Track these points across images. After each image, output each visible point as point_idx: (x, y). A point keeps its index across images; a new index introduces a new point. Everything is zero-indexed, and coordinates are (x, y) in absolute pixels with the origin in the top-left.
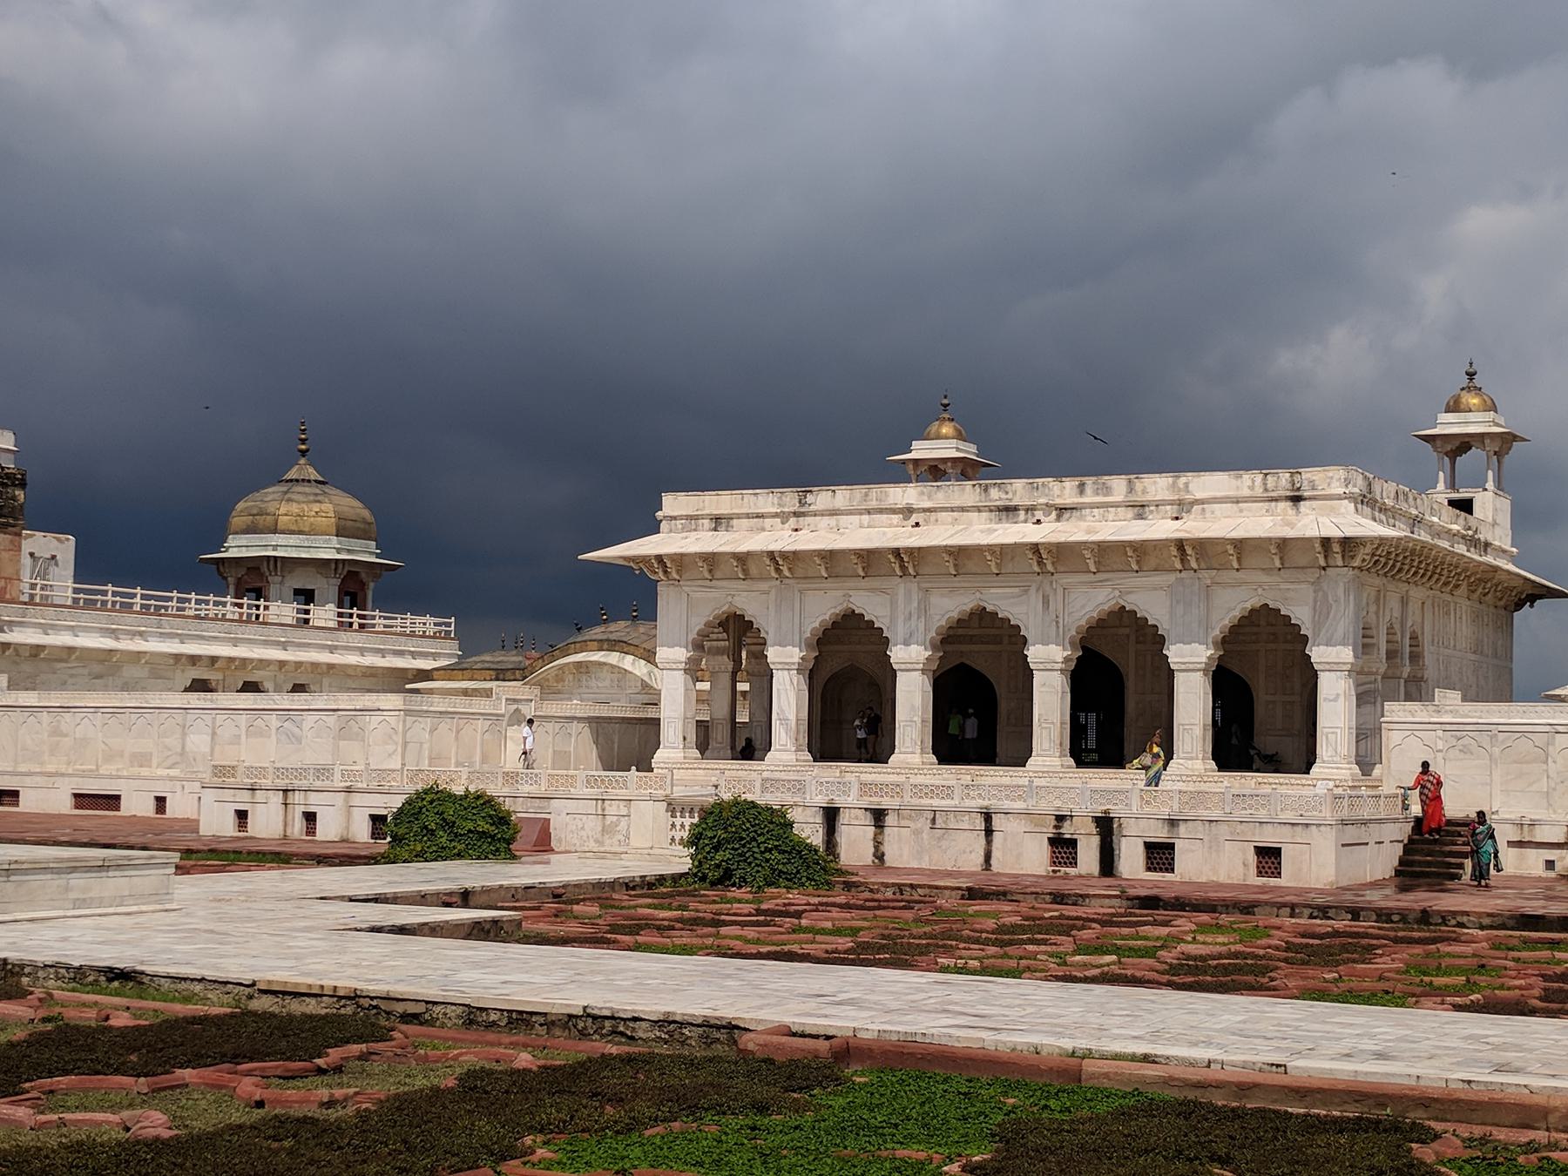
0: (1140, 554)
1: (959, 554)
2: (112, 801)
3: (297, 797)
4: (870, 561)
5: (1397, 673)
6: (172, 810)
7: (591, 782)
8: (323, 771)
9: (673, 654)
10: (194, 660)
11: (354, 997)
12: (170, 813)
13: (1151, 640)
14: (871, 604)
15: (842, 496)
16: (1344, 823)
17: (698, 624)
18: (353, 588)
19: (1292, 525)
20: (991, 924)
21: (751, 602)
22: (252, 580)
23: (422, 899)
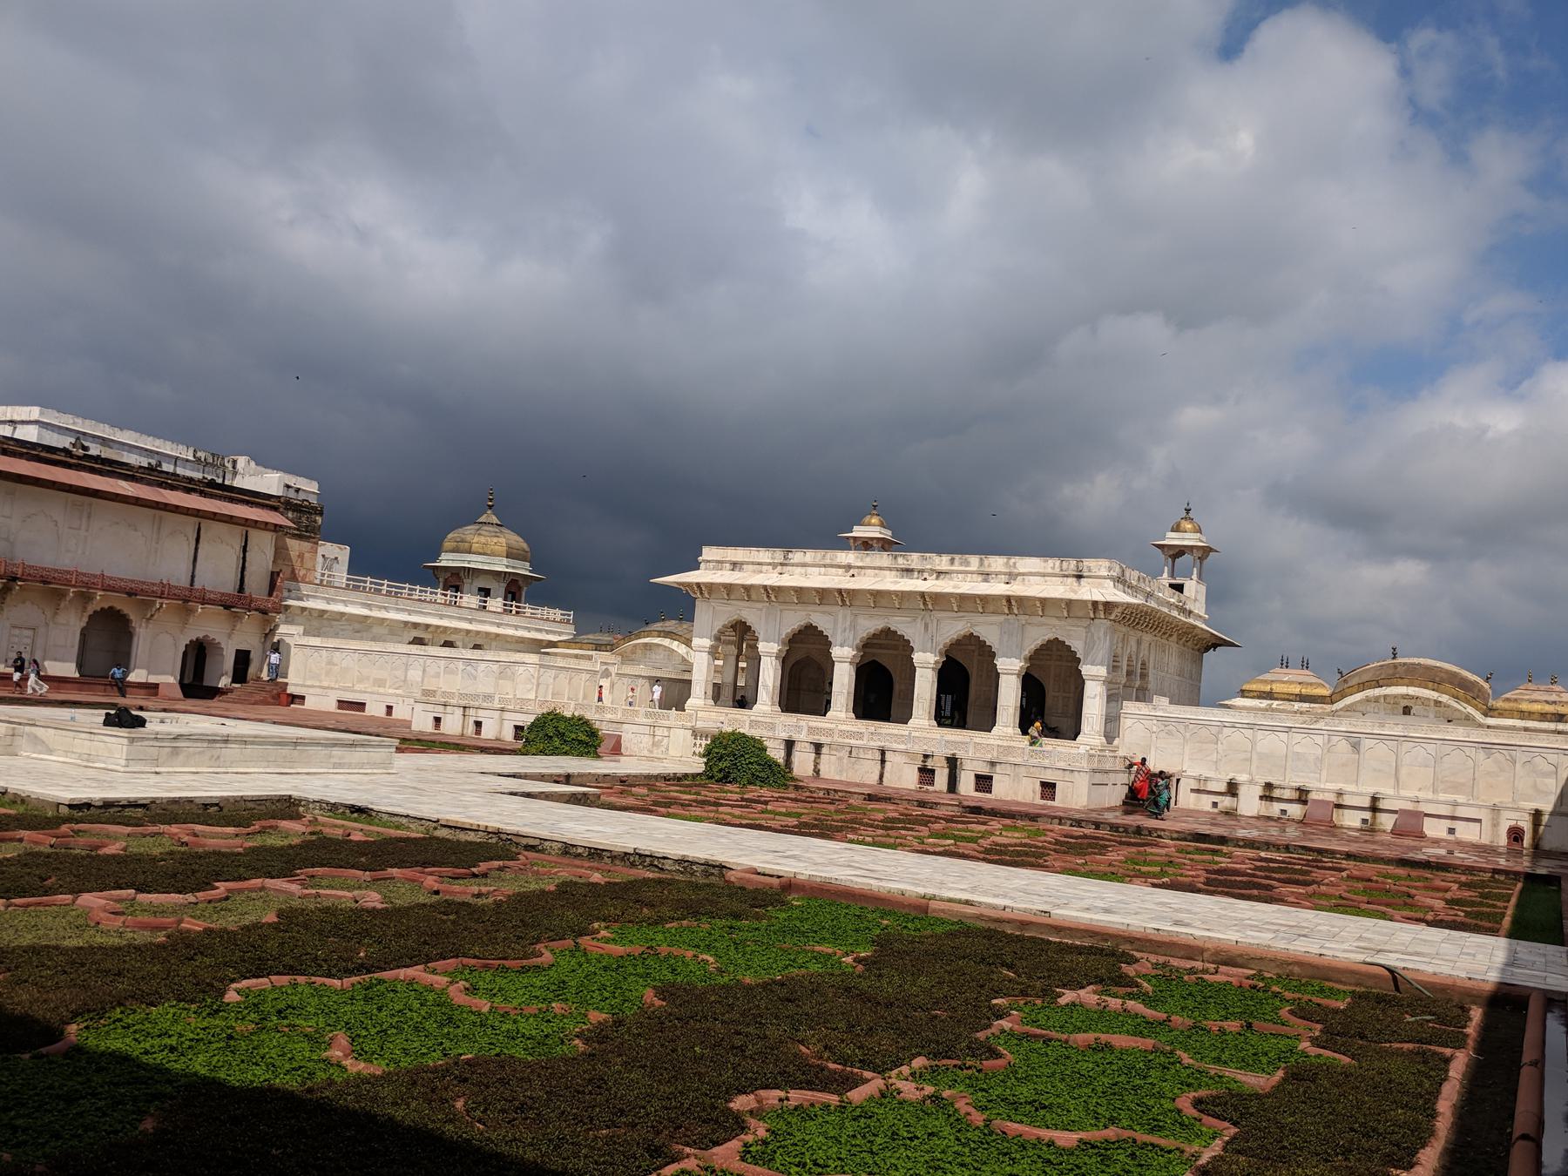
0: (983, 603)
1: (877, 595)
2: (361, 706)
3: (472, 712)
4: (823, 595)
5: (1131, 684)
6: (396, 714)
7: (647, 715)
8: (489, 697)
9: (703, 642)
10: (416, 625)
11: (498, 833)
12: (394, 715)
13: (986, 654)
14: (822, 621)
15: (810, 556)
16: (1094, 771)
17: (718, 625)
18: (514, 589)
19: (1075, 592)
20: (880, 816)
21: (752, 615)
22: (454, 581)
23: (542, 778)
